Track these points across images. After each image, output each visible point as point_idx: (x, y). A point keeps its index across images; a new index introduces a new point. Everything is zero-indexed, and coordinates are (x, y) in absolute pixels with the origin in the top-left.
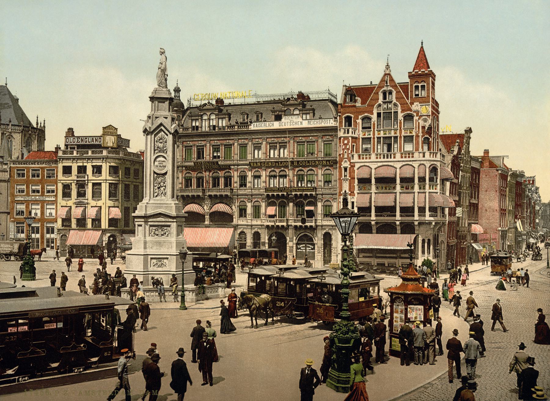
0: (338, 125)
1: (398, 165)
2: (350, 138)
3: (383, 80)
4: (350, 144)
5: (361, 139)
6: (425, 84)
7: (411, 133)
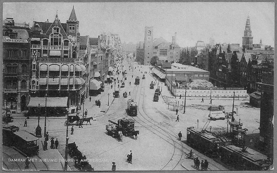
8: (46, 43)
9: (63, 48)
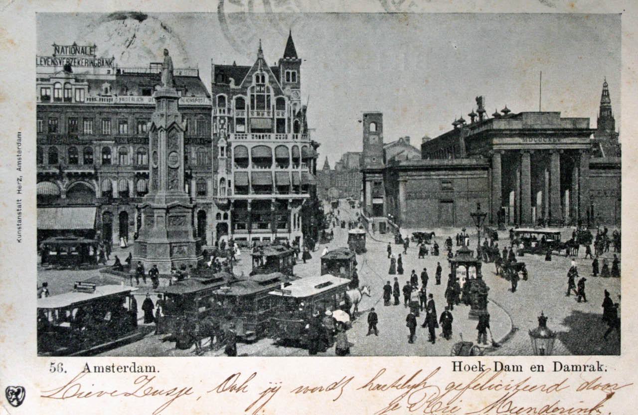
0: (211, 103)
1: (273, 146)
2: (226, 118)
3: (257, 64)
4: (226, 124)
5: (235, 121)
6: (296, 71)
7: (283, 115)
8: (240, 104)
9: (276, 114)
